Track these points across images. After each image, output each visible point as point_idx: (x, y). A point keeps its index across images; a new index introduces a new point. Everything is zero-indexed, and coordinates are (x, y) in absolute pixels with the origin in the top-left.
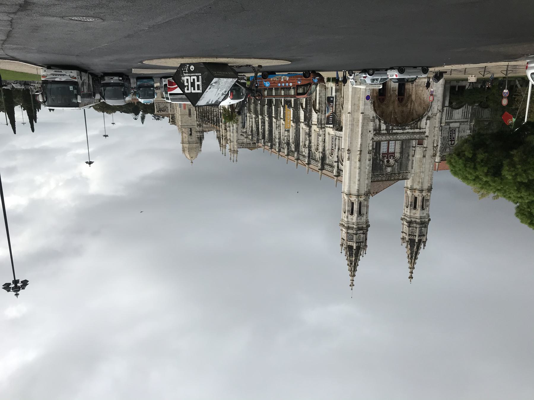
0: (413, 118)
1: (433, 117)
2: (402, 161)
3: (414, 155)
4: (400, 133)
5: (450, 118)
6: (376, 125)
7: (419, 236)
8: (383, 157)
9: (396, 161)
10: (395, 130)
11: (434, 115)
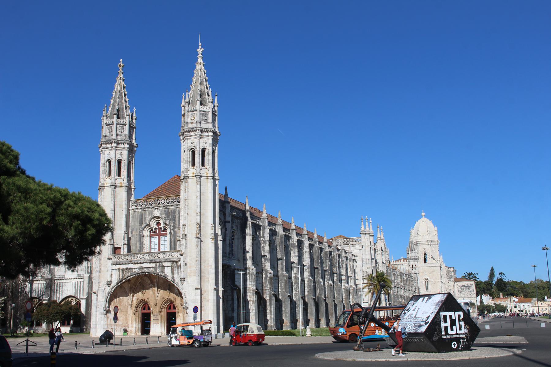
0: (129, 283)
1: (103, 285)
2: (140, 225)
5: (78, 284)
6: (178, 273)
8: (165, 230)
9: (149, 225)
10: (152, 267)
11: (102, 288)
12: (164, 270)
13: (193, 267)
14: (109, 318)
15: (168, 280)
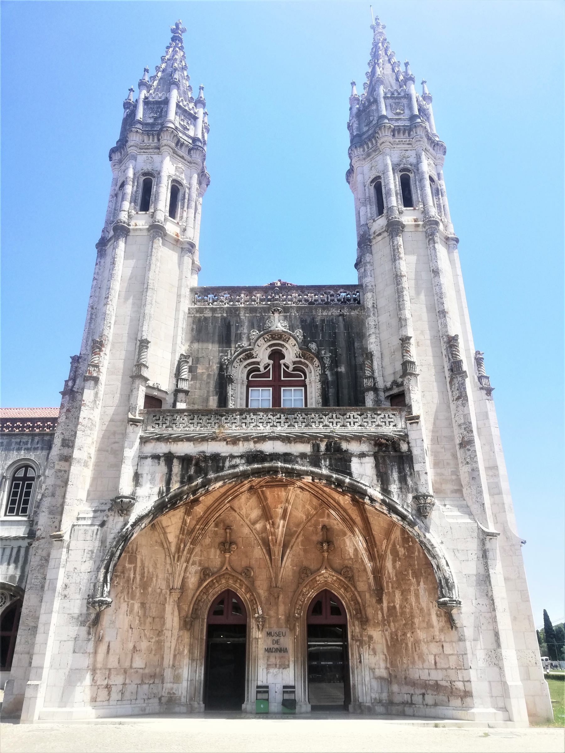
3: (179, 363)
6: (403, 480)
7: (166, 102)
8: (299, 369)
10: (303, 456)
12: (349, 467)
13: (448, 464)
14: (101, 641)
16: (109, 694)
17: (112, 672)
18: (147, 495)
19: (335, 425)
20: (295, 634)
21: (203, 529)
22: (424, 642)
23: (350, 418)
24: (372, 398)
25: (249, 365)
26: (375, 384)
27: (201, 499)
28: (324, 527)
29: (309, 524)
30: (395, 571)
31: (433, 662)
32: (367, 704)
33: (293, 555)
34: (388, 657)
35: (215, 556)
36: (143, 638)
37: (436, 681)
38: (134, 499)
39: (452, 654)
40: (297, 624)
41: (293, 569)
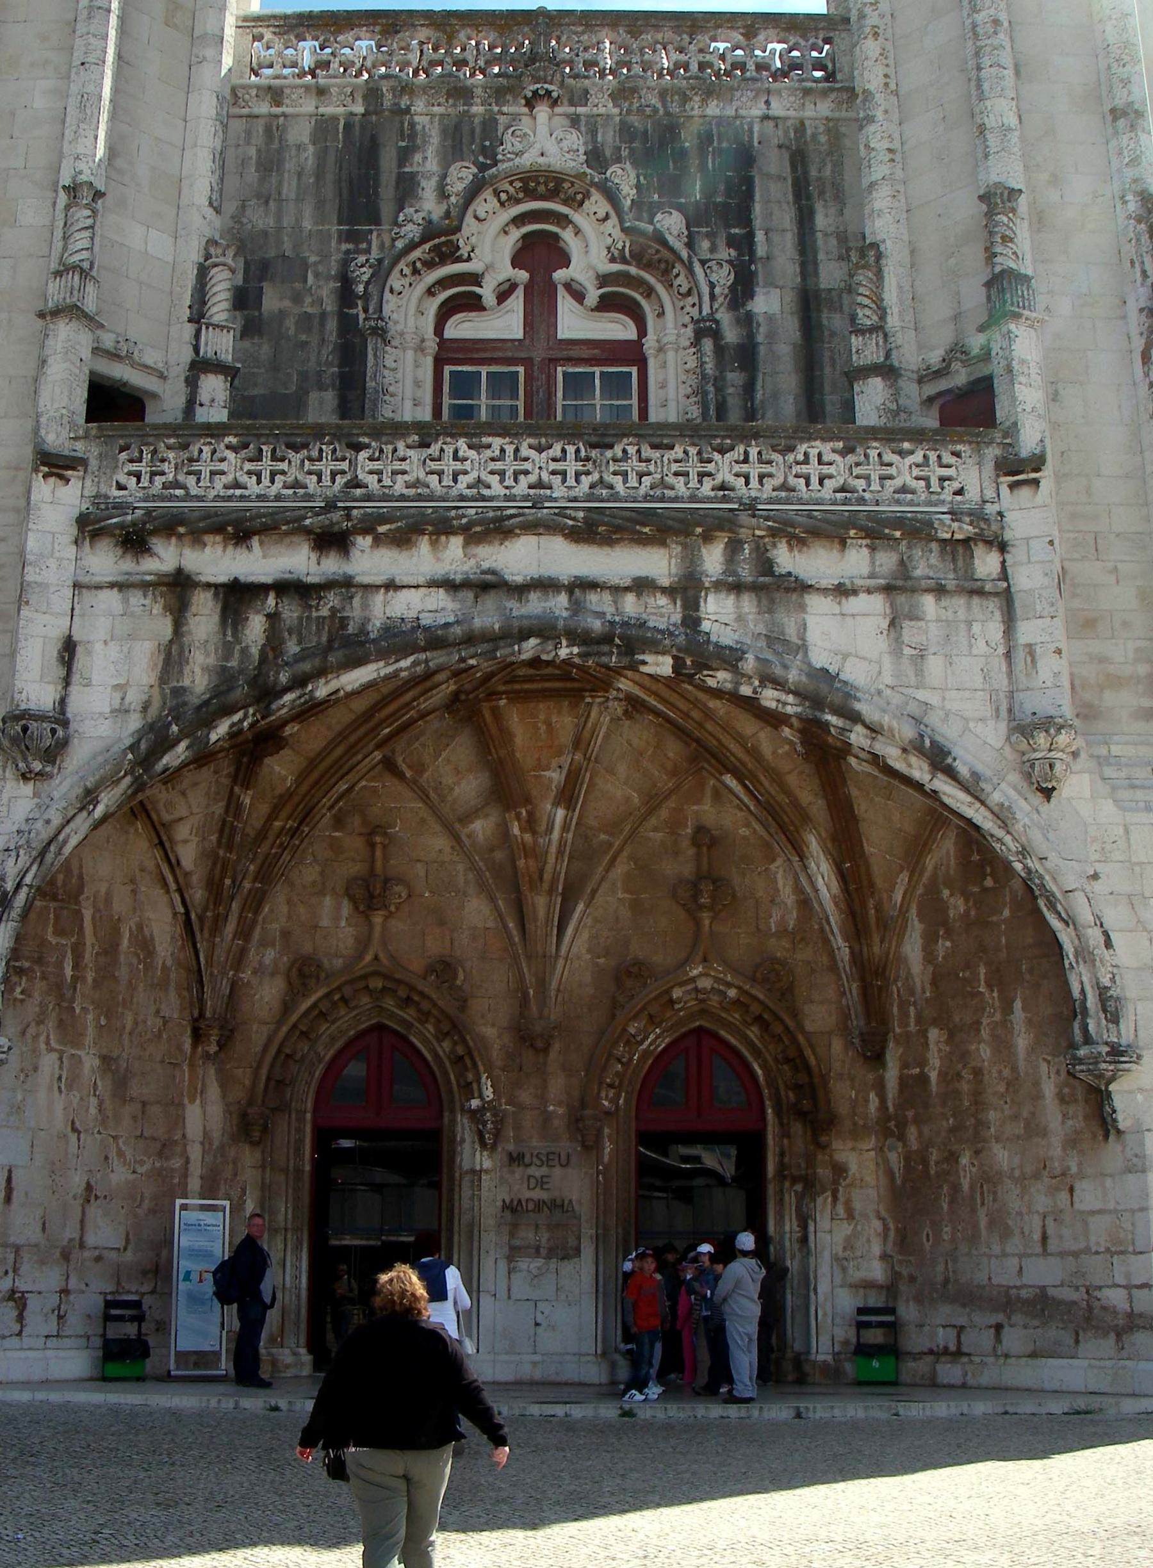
3: (203, 272)
4: (533, 527)
10: (642, 586)
13: (1125, 624)
15: (858, 737)
16: (20, 1318)
17: (26, 1256)
18: (108, 710)
19: (754, 483)
20: (599, 1160)
21: (294, 833)
22: (1012, 1177)
23: (806, 461)
24: (879, 400)
25: (443, 283)
26: (888, 355)
27: (289, 730)
28: (700, 829)
29: (653, 821)
30: (931, 968)
31: (1037, 1236)
32: (820, 1358)
33: (596, 920)
34: (892, 1226)
35: (336, 918)
36: (115, 1162)
37: (1043, 1288)
38: (65, 724)
39: (1100, 1212)
40: (606, 1131)
41: (597, 965)
